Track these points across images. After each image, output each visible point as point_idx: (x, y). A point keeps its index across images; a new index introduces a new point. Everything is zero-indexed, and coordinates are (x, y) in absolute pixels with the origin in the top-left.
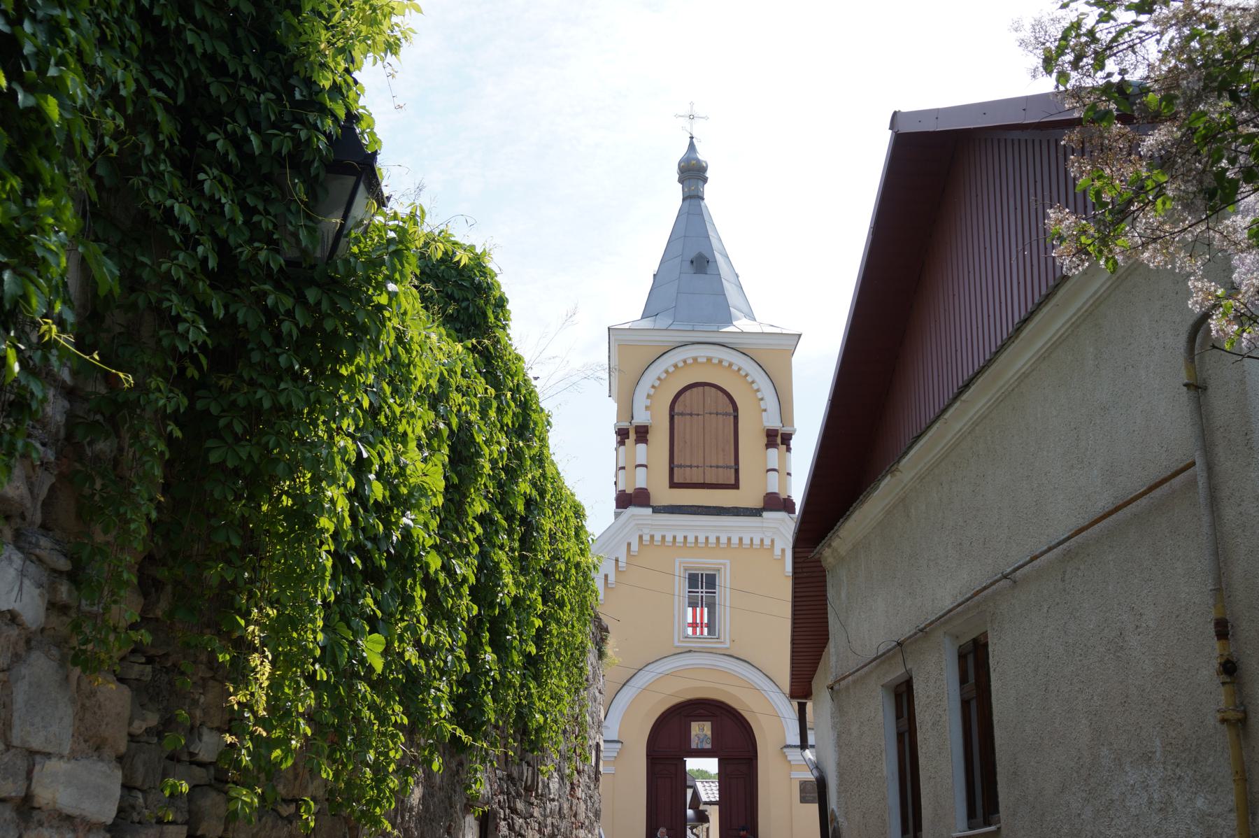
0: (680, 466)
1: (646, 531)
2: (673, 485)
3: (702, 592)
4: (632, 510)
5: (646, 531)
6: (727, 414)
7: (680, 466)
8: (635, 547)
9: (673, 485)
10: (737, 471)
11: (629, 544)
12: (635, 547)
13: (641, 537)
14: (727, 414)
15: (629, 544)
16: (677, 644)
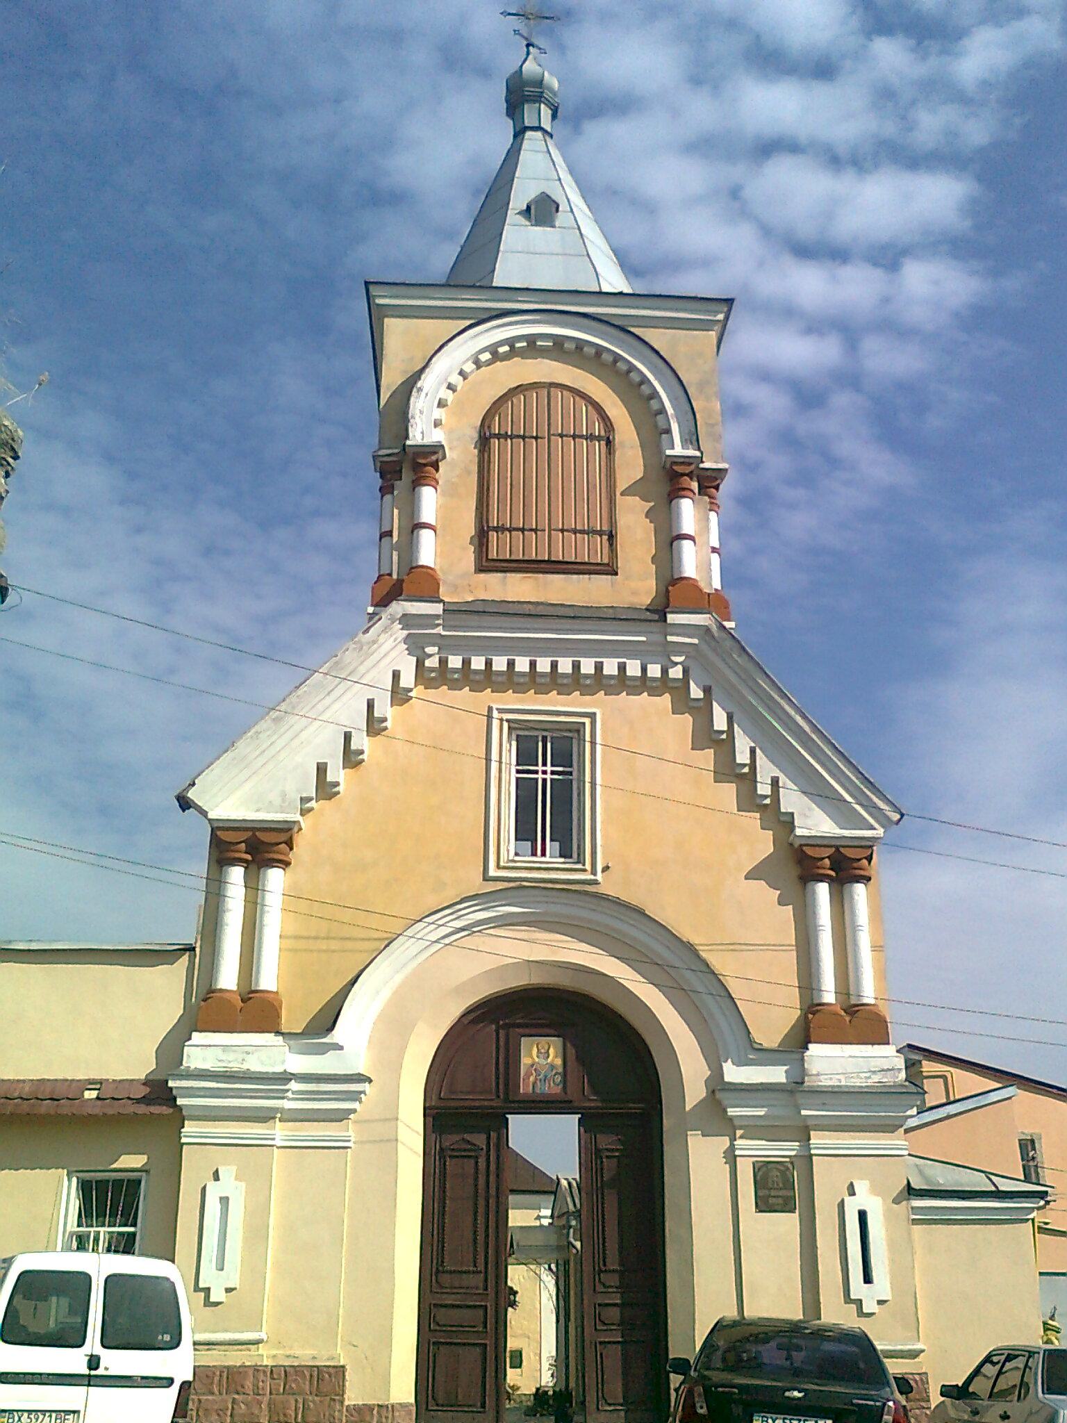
0: (500, 529)
1: (429, 650)
2: (485, 564)
3: (545, 772)
4: (400, 607)
5: (430, 650)
6: (591, 437)
7: (500, 529)
8: (407, 680)
9: (485, 564)
10: (612, 537)
11: (396, 675)
12: (407, 680)
13: (420, 665)
14: (591, 437)
15: (396, 675)
16: (493, 872)
